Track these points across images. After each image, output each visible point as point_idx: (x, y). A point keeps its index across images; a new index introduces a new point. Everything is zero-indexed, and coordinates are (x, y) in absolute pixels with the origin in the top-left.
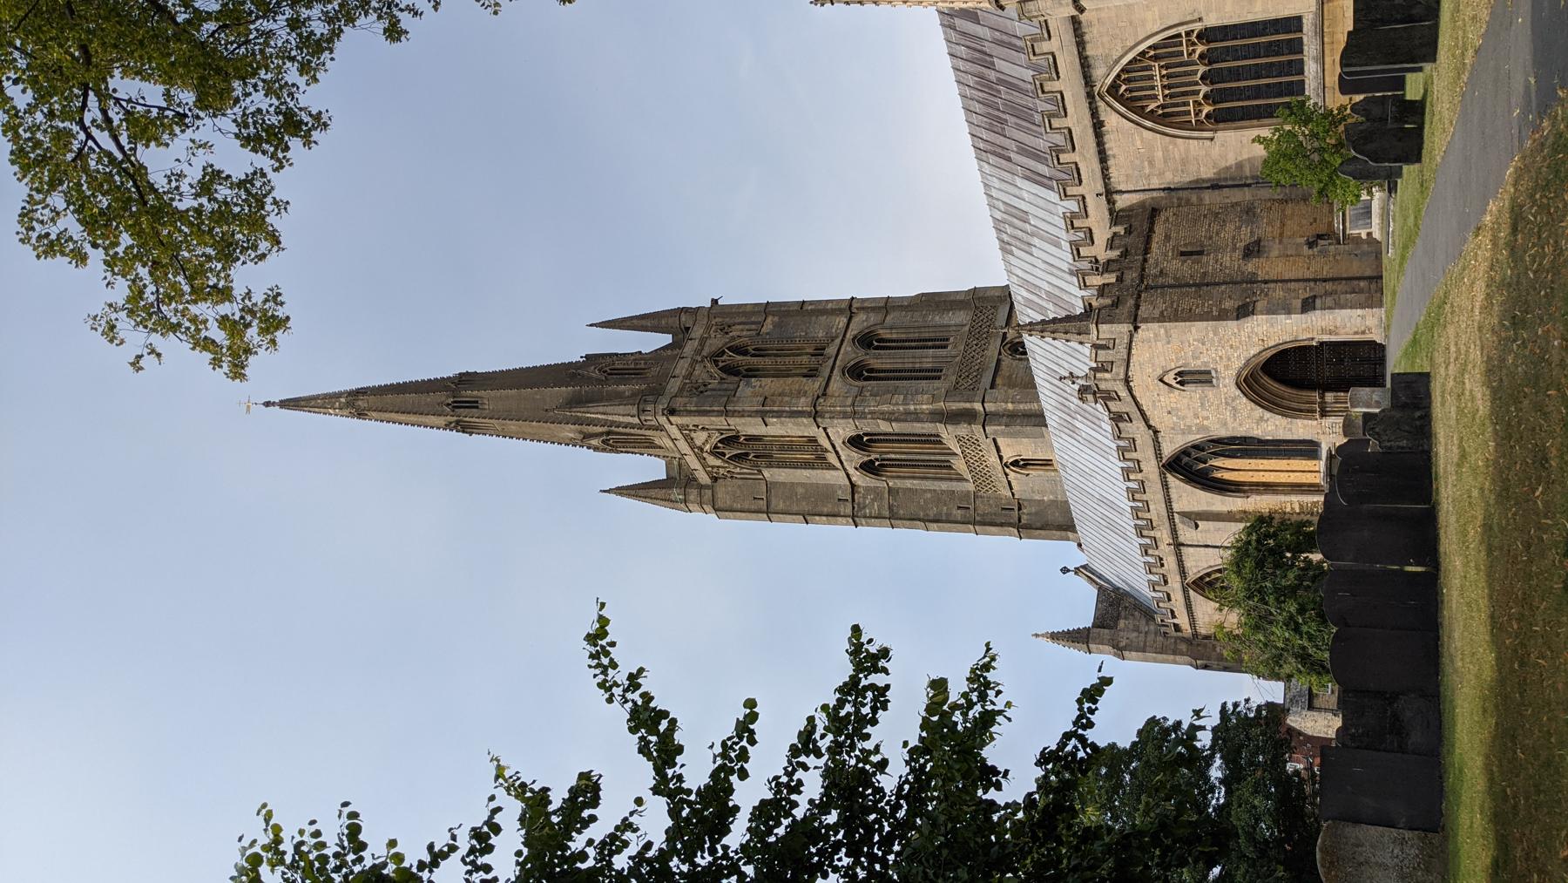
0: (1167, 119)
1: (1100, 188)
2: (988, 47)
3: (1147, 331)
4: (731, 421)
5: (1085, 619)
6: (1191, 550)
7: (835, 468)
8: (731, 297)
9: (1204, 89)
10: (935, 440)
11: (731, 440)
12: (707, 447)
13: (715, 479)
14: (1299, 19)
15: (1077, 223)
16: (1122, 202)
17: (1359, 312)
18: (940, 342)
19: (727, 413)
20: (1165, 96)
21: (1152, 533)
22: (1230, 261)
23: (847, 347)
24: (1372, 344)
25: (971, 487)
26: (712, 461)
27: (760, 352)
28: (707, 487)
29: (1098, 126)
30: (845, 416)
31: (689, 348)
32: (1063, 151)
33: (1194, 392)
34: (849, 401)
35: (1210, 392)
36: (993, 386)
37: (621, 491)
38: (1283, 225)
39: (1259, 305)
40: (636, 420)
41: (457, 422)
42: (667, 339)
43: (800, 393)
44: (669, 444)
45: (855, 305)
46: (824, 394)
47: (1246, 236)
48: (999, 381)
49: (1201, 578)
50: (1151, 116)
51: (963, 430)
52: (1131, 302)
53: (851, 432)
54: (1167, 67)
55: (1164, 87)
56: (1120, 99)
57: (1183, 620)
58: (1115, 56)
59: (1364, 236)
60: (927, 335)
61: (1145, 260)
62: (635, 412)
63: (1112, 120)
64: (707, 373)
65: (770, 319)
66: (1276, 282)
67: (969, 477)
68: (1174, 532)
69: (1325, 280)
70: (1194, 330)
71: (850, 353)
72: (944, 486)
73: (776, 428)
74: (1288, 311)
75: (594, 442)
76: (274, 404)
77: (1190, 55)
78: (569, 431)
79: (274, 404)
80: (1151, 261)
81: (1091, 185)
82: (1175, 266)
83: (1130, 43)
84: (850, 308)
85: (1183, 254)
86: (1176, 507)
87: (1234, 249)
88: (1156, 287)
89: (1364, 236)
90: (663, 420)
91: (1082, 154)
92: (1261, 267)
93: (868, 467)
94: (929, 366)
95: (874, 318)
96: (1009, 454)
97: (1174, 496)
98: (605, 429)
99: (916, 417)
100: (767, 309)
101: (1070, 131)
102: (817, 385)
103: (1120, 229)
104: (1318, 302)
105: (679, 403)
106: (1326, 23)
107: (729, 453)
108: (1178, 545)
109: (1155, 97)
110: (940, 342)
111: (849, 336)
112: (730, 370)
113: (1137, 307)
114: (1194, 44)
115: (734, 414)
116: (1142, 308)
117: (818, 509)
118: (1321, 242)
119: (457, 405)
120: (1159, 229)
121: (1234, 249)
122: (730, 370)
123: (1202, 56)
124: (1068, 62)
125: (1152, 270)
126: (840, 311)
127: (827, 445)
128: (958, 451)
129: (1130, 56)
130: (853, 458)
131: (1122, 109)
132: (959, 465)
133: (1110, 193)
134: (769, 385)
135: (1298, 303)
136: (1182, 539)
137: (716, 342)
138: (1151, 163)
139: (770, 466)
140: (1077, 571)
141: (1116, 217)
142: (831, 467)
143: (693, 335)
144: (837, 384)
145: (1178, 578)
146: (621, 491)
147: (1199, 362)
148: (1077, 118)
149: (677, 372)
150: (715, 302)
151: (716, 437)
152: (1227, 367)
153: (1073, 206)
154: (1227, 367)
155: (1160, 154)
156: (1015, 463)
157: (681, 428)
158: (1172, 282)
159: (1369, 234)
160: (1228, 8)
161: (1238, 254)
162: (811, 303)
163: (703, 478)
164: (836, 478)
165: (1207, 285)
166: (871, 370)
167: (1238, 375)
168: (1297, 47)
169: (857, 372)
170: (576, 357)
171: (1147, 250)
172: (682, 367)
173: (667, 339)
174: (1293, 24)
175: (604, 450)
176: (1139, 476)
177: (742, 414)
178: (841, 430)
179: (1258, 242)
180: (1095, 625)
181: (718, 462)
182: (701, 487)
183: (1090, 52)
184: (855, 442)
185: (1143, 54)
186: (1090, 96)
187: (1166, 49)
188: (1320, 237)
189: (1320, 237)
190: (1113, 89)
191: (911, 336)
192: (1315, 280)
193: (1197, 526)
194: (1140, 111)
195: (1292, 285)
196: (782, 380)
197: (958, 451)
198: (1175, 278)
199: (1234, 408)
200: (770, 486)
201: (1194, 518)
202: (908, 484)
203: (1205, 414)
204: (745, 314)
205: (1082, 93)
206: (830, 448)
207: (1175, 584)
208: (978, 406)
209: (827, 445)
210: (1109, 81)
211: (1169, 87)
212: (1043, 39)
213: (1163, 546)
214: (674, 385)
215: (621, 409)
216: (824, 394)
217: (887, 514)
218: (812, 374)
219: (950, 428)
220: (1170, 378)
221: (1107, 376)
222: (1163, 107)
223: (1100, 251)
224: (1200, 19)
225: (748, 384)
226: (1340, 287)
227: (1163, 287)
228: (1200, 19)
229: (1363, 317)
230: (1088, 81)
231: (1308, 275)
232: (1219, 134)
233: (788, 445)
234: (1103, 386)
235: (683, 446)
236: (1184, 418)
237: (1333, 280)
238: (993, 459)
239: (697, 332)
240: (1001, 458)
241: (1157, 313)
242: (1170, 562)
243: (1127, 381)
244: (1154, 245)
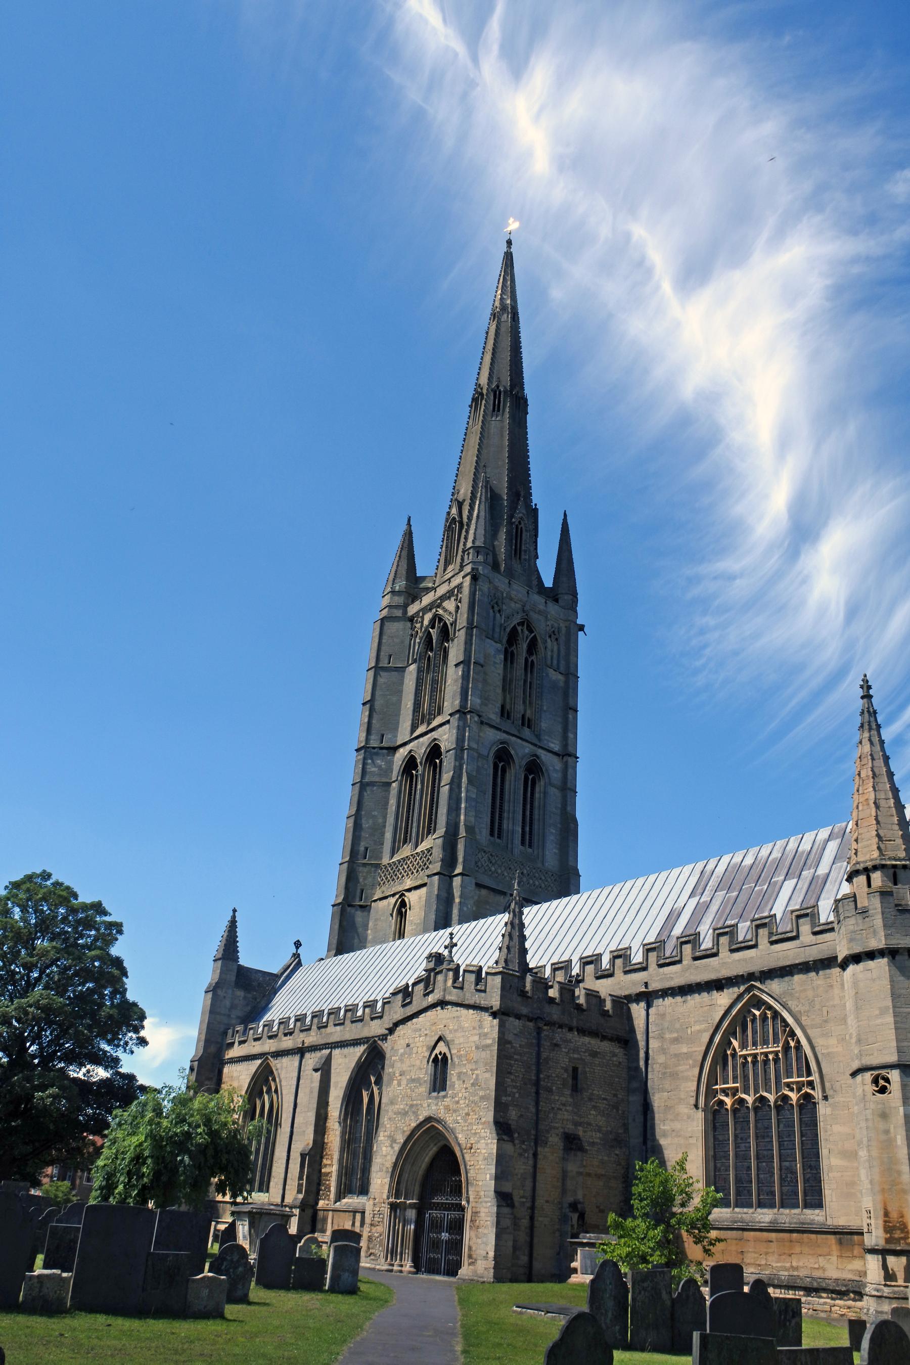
0: (720, 1058)
1: (654, 986)
2: (807, 874)
3: (491, 1025)
4: (463, 632)
5: (246, 959)
6: (297, 1064)
7: (413, 730)
8: (586, 648)
9: (750, 1099)
10: (430, 829)
11: (445, 634)
12: (441, 612)
13: (411, 620)
14: (819, 1205)
15: (619, 962)
16: (638, 1010)
17: (492, 1254)
18: (528, 839)
19: (470, 628)
20: (745, 1057)
21: (314, 1027)
22: (562, 1116)
23: (528, 749)
24: (458, 1265)
25: (385, 860)
26: (428, 617)
27: (529, 666)
28: (405, 612)
29: (718, 985)
30: (460, 740)
31: (539, 600)
32: (694, 949)
33: (425, 1072)
34: (475, 746)
35: (424, 1089)
36: (478, 885)
37: (409, 536)
38: (599, 1176)
39: (509, 1148)
40: (469, 544)
41: (481, 394)
42: (548, 582)
43: (485, 700)
44: (447, 577)
45: (570, 760)
46: (482, 723)
47: (588, 1136)
48: (484, 892)
49: (272, 1073)
50: (726, 1043)
51: (438, 854)
52: (524, 1011)
54: (776, 1060)
55: (755, 1056)
56: (745, 1010)
58: (792, 1004)
59: (573, 1265)
60: (536, 827)
61: (571, 1029)
62: (478, 544)
63: (723, 999)
65: (560, 677)
66: (535, 1167)
67: (394, 860)
68: (314, 1048)
69: (532, 1218)
70: (488, 1075)
72: (388, 835)
73: (453, 675)
74: (498, 1178)
75: (454, 511)
77: (788, 1085)
78: (465, 490)
80: (569, 1036)
81: (658, 978)
82: (561, 1060)
83: (804, 1020)
84: (568, 755)
85: (575, 1070)
86: (336, 1052)
87: (576, 1124)
88: (539, 1039)
89: (573, 1265)
90: (468, 569)
91: (689, 967)
92: (551, 1153)
93: (411, 763)
94: (505, 826)
95: (556, 777)
96: (413, 898)
97: (346, 1051)
98: (465, 520)
99: (454, 809)
100: (571, 676)
101: (715, 955)
102: (493, 717)
103: (608, 1006)
104: (506, 1210)
105: (484, 586)
106: (813, 1236)
108: (301, 1051)
109: (744, 1046)
110: (528, 839)
111: (540, 752)
112: (513, 637)
113: (518, 1017)
114: (799, 1090)
115: (469, 635)
116: (517, 1022)
117: (375, 716)
118: (575, 1216)
119: (496, 393)
120: (606, 1046)
121: (576, 1124)
122: (513, 637)
123: (785, 1098)
124: (787, 954)
125: (559, 1035)
126: (565, 745)
127: (435, 723)
128: (419, 850)
129: (790, 1020)
130: (420, 748)
131: (734, 1012)
132: (406, 851)
133: (648, 997)
134: (496, 671)
135: (507, 1188)
136: (307, 1055)
137: (541, 627)
138: (676, 1040)
139: (419, 671)
140: (296, 956)
141: (623, 1003)
142: (414, 728)
143: (550, 604)
144: (491, 735)
145: (273, 1049)
146: (409, 536)
147: (454, 1079)
148: (729, 964)
149: (515, 587)
150: (581, 628)
151: (449, 619)
152: (447, 1108)
153: (637, 958)
154: (447, 1108)
155: (685, 1050)
156: (403, 904)
157: (459, 587)
158: (544, 1055)
159: (575, 1271)
160: (837, 1128)
161: (570, 1127)
162: (575, 718)
163: (413, 609)
164: (404, 734)
165: (537, 1093)
166: (504, 771)
167: (439, 1121)
168: (788, 1202)
169: (503, 757)
170: (537, 498)
171: (582, 1031)
172: (518, 590)
173: (548, 582)
174: (814, 1198)
175: (447, 520)
176: (367, 1018)
177: (468, 643)
178: (446, 737)
179: (581, 1149)
180: (241, 968)
181: (426, 622)
182: (405, 607)
183: (797, 978)
184: (435, 752)
185: (792, 1034)
186: (751, 976)
187: (794, 1057)
188: (582, 1216)
189: (582, 1216)
190: (758, 1003)
191: (536, 812)
192: (533, 1208)
193: (316, 1070)
194: (731, 1032)
195: (529, 1184)
196: (500, 684)
197: (419, 850)
198: (547, 1060)
199: (405, 1114)
200: (402, 670)
201: (325, 1070)
202: (393, 802)
203: (404, 1082)
204: (568, 654)
205: (755, 968)
206: (431, 726)
207: (269, 1046)
208: (459, 869)
209: (435, 723)
210: (765, 997)
211: (755, 1062)
212: (813, 925)
213: (302, 1036)
214: (501, 583)
215: (481, 531)
216: (482, 723)
217: (366, 780)
218: (504, 713)
219: (440, 841)
220: (441, 1048)
221: (450, 982)
222: (734, 1055)
223: (591, 983)
224: (826, 1098)
225: (498, 651)
226: (523, 1237)
227: (539, 1045)
228: (826, 1098)
229: (486, 1258)
230: (768, 975)
231: (539, 1202)
232: (700, 1115)
233: (437, 687)
234: (440, 978)
235: (442, 590)
236: (401, 1060)
237: (532, 1227)
238: (409, 883)
239: (553, 609)
240: (409, 890)
241: (510, 1037)
242: (287, 1043)
243: (442, 1003)
244: (587, 1040)
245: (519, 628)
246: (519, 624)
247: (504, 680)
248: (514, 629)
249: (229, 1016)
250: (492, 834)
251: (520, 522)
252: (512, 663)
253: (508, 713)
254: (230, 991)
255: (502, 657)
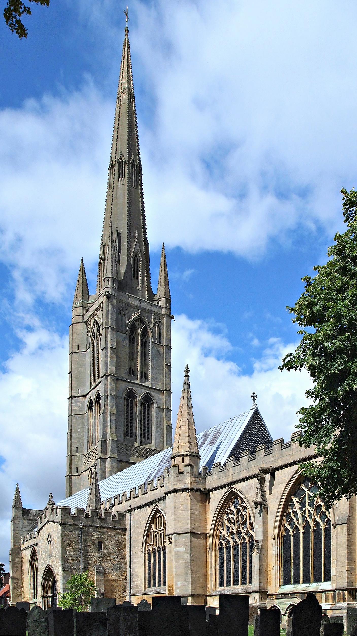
5: (26, 505)
12: (97, 319)
53: (102, 394)
57: (26, 545)
107: (95, 330)
112: (133, 328)
122: (133, 328)
151: (100, 323)
166: (132, 402)
225: (124, 338)
245: (136, 323)
246: (136, 321)
247: (130, 353)
249: (22, 531)
250: (127, 436)
253: (133, 372)
254: (21, 521)
255: (127, 341)
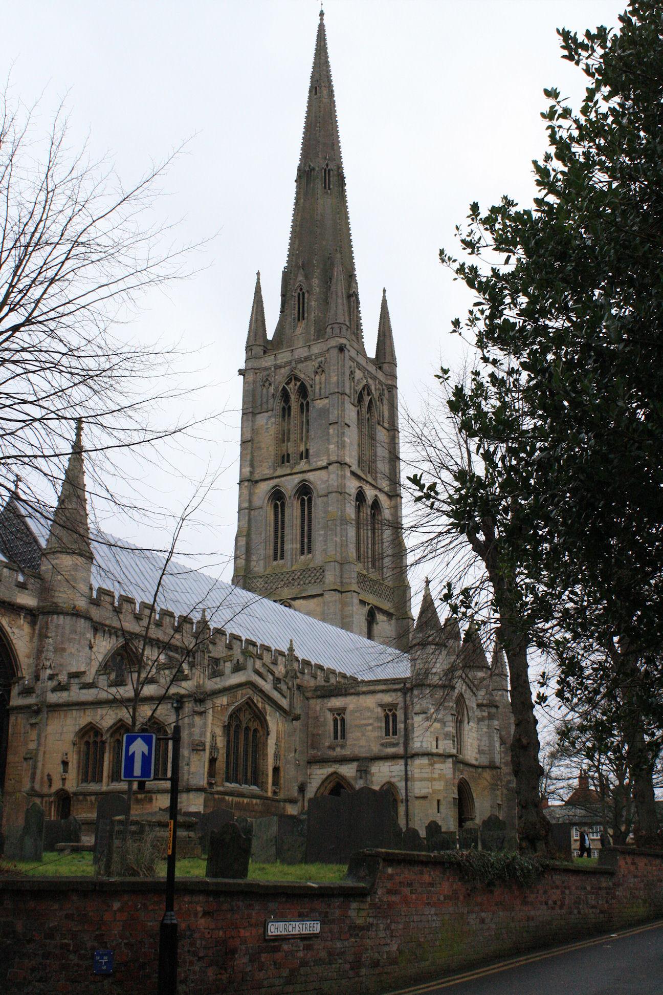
46: (257, 482)
64: (280, 377)
71: (289, 485)
76: (322, 19)
79: (322, 19)
112: (285, 396)
122: (285, 396)
169: (277, 496)
216: (257, 482)
246: (288, 383)
248: (284, 389)
251: (301, 290)
252: (289, 415)
